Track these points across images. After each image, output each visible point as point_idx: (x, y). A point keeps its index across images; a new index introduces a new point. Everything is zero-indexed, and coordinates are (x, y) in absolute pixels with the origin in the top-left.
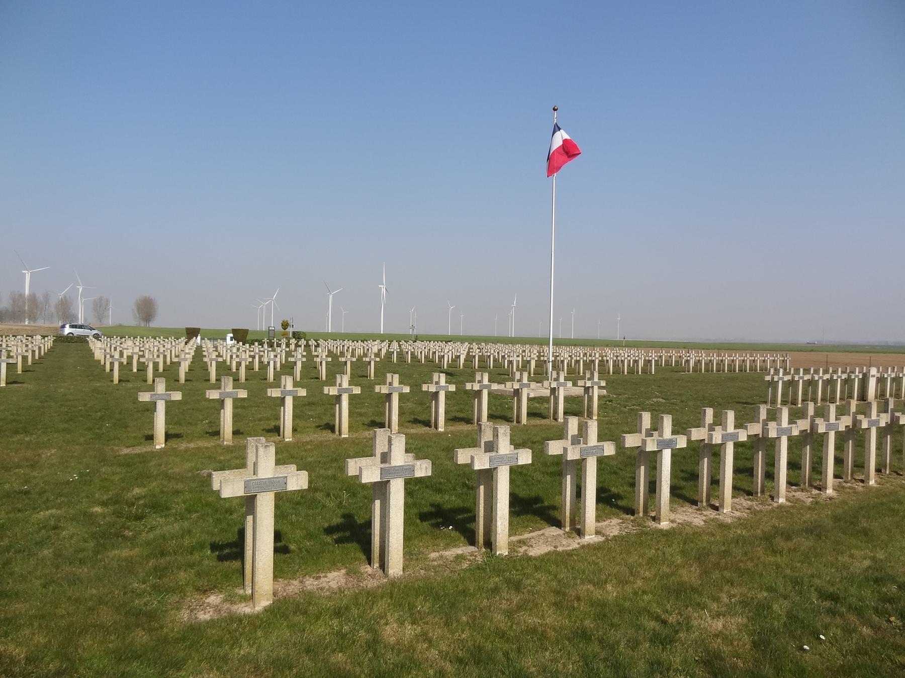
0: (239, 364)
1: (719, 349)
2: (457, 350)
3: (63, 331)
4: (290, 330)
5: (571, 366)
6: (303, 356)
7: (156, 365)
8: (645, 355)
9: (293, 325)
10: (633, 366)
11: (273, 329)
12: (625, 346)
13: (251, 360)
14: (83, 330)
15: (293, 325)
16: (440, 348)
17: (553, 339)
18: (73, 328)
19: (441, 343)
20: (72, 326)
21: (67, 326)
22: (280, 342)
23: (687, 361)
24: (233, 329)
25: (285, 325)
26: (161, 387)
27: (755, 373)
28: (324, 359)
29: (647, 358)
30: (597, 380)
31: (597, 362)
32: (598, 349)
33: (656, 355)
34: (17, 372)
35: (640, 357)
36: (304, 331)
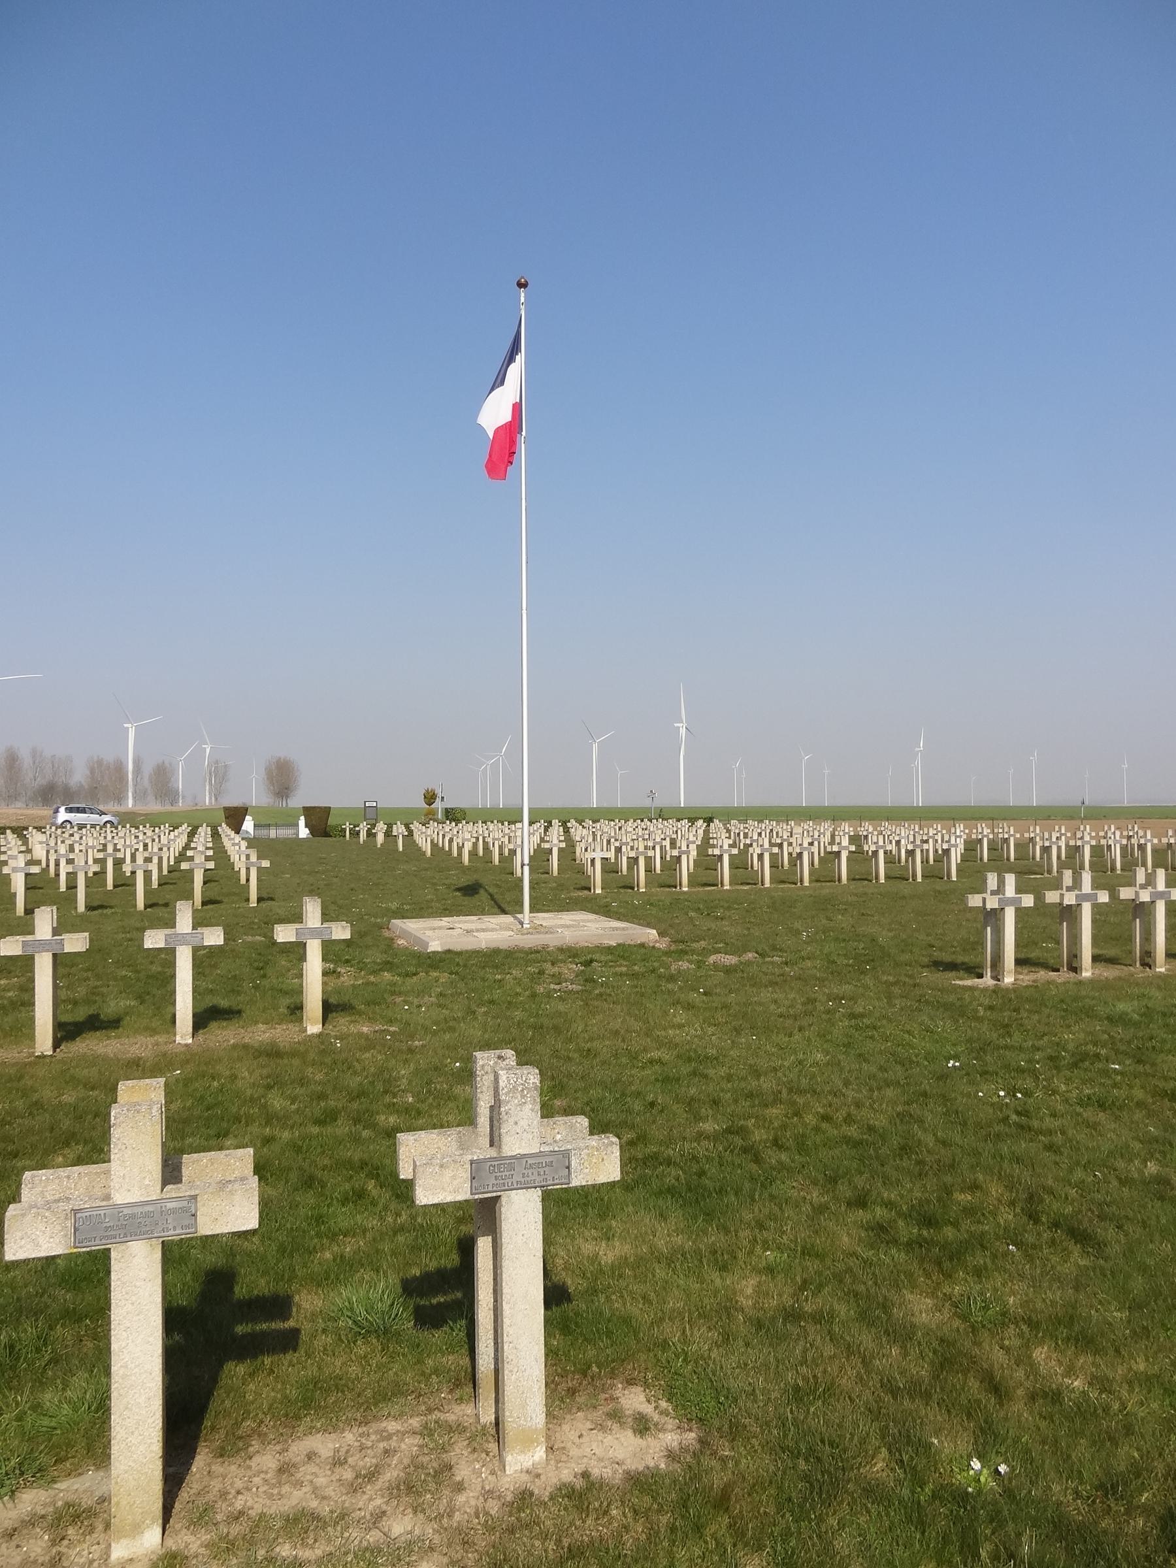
0: (72, 877)
1: (953, 819)
2: (777, 833)
3: (55, 818)
4: (439, 805)
5: (927, 861)
6: (208, 859)
7: (148, 874)
8: (1069, 835)
9: (443, 798)
10: (907, 861)
11: (375, 804)
12: (1086, 818)
13: (96, 868)
14: (87, 815)
15: (443, 798)
16: (647, 832)
17: (530, 810)
18: (71, 812)
19: (649, 823)
20: (70, 810)
21: (62, 809)
22: (357, 829)
23: (1046, 850)
24: (304, 807)
25: (430, 798)
26: (44, 921)
27: (798, 889)
28: (253, 864)
29: (1072, 843)
30: (318, 924)
31: (844, 855)
32: (939, 826)
33: (1093, 834)
34: (59, 889)
35: (953, 842)
36: (462, 806)
